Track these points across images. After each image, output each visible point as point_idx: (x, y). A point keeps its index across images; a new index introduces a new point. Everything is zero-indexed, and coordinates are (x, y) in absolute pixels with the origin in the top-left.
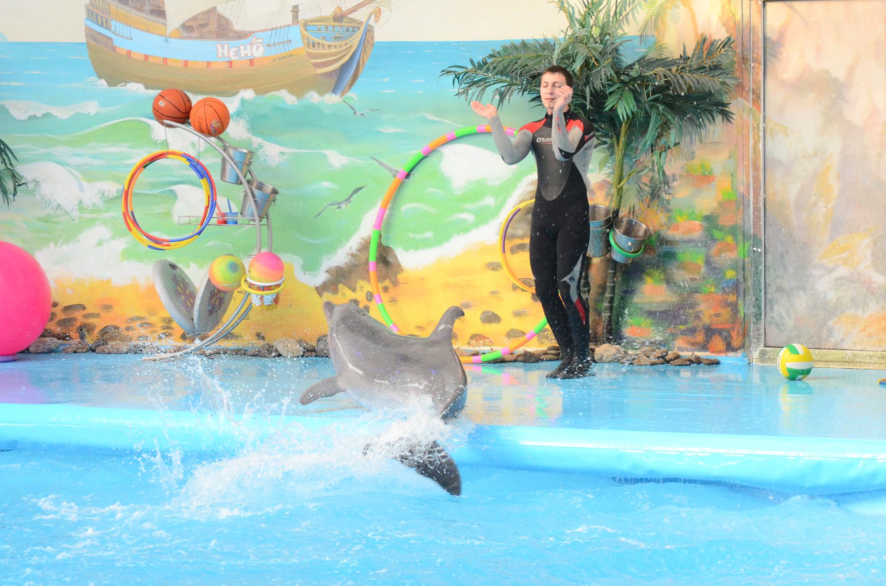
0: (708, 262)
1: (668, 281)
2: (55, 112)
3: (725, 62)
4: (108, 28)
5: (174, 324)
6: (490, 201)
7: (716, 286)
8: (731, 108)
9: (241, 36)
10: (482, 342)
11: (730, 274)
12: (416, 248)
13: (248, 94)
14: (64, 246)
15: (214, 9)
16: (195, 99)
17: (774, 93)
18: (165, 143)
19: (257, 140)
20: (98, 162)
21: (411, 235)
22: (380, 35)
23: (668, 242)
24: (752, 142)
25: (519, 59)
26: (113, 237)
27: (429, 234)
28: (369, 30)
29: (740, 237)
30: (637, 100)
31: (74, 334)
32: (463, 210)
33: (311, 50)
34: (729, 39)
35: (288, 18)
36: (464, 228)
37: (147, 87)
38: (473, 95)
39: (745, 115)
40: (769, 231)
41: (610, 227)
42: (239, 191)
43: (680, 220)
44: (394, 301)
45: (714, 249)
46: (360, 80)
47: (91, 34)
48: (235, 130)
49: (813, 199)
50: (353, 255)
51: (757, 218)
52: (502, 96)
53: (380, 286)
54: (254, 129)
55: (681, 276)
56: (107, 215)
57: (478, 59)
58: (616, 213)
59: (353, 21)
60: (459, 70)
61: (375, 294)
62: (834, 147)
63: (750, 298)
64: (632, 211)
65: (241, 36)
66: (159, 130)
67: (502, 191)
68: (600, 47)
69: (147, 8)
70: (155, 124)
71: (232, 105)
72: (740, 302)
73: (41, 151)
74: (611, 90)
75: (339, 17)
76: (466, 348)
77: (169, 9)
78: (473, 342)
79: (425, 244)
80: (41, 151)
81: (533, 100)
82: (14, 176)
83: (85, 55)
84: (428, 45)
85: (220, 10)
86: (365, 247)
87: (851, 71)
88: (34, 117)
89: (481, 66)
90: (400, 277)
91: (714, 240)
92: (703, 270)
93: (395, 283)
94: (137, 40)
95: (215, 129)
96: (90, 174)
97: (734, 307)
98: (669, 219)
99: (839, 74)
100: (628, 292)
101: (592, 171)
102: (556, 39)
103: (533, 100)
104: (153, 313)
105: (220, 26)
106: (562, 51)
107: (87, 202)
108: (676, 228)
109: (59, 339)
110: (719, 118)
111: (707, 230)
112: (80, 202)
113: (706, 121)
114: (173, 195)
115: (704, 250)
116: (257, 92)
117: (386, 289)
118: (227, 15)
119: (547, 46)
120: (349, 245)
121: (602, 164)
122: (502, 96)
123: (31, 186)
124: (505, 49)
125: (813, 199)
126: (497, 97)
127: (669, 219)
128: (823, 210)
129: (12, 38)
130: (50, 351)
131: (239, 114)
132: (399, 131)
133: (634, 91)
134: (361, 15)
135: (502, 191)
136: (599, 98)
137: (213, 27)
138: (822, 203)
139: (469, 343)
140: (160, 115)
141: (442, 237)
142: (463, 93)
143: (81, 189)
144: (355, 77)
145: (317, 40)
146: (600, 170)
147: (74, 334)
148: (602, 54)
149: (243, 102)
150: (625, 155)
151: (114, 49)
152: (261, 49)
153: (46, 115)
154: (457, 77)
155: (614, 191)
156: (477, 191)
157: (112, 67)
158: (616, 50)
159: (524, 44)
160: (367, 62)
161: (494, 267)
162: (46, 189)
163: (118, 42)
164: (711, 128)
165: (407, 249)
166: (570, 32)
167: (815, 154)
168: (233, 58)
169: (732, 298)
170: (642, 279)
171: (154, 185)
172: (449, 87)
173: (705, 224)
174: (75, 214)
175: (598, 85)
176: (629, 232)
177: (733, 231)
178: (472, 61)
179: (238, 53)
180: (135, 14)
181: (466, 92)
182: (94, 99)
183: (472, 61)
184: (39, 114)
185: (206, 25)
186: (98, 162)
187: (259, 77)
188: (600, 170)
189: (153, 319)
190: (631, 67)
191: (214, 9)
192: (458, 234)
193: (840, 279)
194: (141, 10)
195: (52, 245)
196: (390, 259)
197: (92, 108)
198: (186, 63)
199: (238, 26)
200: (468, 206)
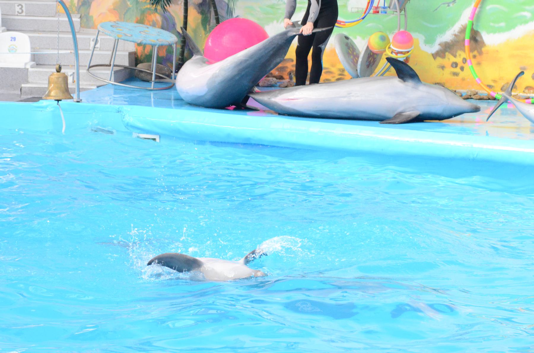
5: (346, 73)
10: (532, 91)
12: (494, 32)
21: (492, 24)
27: (502, 24)
31: (286, 76)
36: (525, 21)
44: (479, 64)
50: (455, 35)
53: (471, 54)
61: (468, 59)
76: (521, 94)
78: (527, 91)
79: (500, 30)
86: (463, 30)
93: (481, 53)
104: (333, 66)
109: (277, 79)
117: (474, 57)
120: (453, 29)
130: (271, 86)
139: (524, 92)
141: (510, 27)
147: (286, 76)
189: (333, 69)
195: (275, 22)
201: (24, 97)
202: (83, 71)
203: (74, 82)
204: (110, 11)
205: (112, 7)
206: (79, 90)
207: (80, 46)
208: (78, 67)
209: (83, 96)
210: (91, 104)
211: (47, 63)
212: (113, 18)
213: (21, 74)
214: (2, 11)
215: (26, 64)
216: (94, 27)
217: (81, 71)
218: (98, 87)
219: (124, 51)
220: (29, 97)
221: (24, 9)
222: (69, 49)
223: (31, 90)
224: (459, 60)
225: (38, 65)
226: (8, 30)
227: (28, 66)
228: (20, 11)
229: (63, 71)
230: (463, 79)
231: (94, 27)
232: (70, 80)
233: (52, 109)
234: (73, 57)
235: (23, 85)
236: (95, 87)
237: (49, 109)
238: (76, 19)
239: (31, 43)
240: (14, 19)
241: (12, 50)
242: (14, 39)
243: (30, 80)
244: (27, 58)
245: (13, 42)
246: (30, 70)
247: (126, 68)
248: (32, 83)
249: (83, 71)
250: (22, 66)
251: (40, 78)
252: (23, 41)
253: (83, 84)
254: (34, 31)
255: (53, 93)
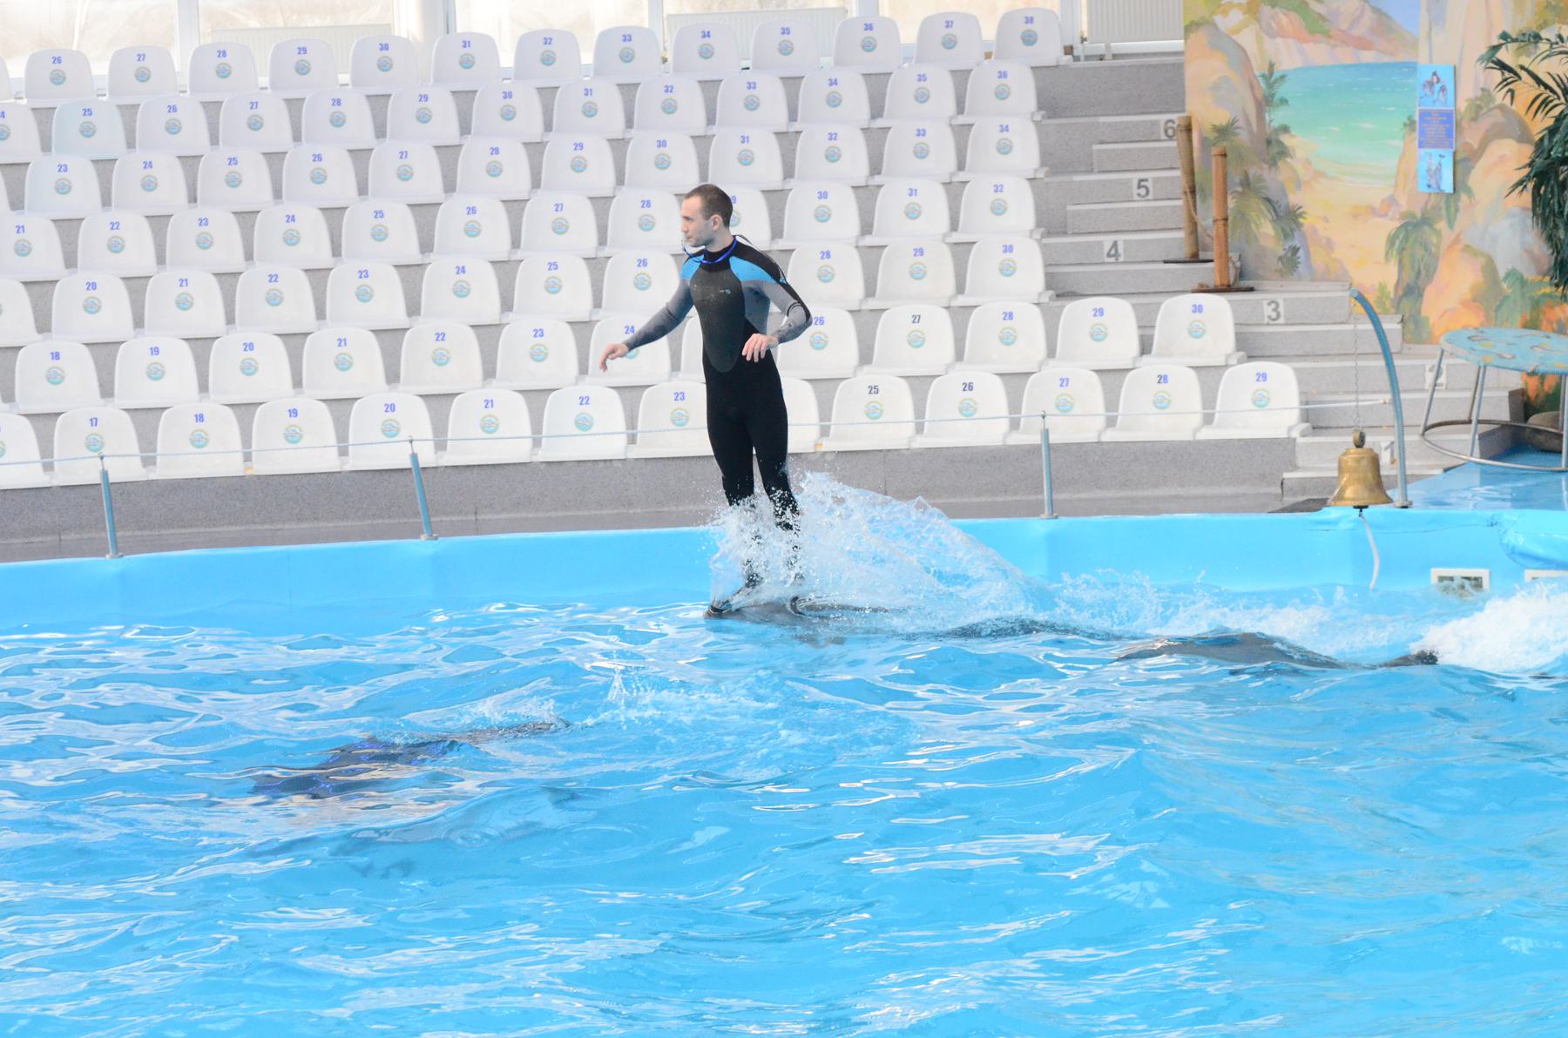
201: (1289, 500)
202: (1412, 438)
203: (1393, 462)
204: (1464, 304)
205: (1469, 296)
206: (1406, 480)
207: (1402, 386)
208: (1402, 426)
209: (1414, 492)
210: (1434, 511)
211: (1334, 424)
212: (1472, 319)
213: (1282, 450)
214: (1235, 317)
215: (1290, 429)
216: (1431, 340)
217: (1407, 438)
218: (1446, 470)
219: (1498, 388)
220: (1301, 499)
221: (1281, 309)
222: (1381, 392)
223: (1303, 485)
225: (1317, 429)
226: (1251, 358)
227: (1295, 434)
228: (1274, 315)
229: (1368, 439)
231: (1431, 340)
232: (1385, 459)
233: (1349, 526)
234: (1389, 412)
235: (1286, 475)
236: (1438, 472)
237: (1341, 526)
238: (1391, 326)
239: (1300, 382)
240: (1263, 334)
241: (1260, 402)
242: (1262, 377)
243: (1300, 463)
244: (1293, 416)
245: (1261, 384)
246: (1300, 440)
247: (1504, 426)
248: (1305, 469)
249: (1412, 438)
250: (1282, 434)
251: (1321, 459)
252: (1283, 379)
253: (1414, 465)
254: (1304, 356)
255: (1349, 493)
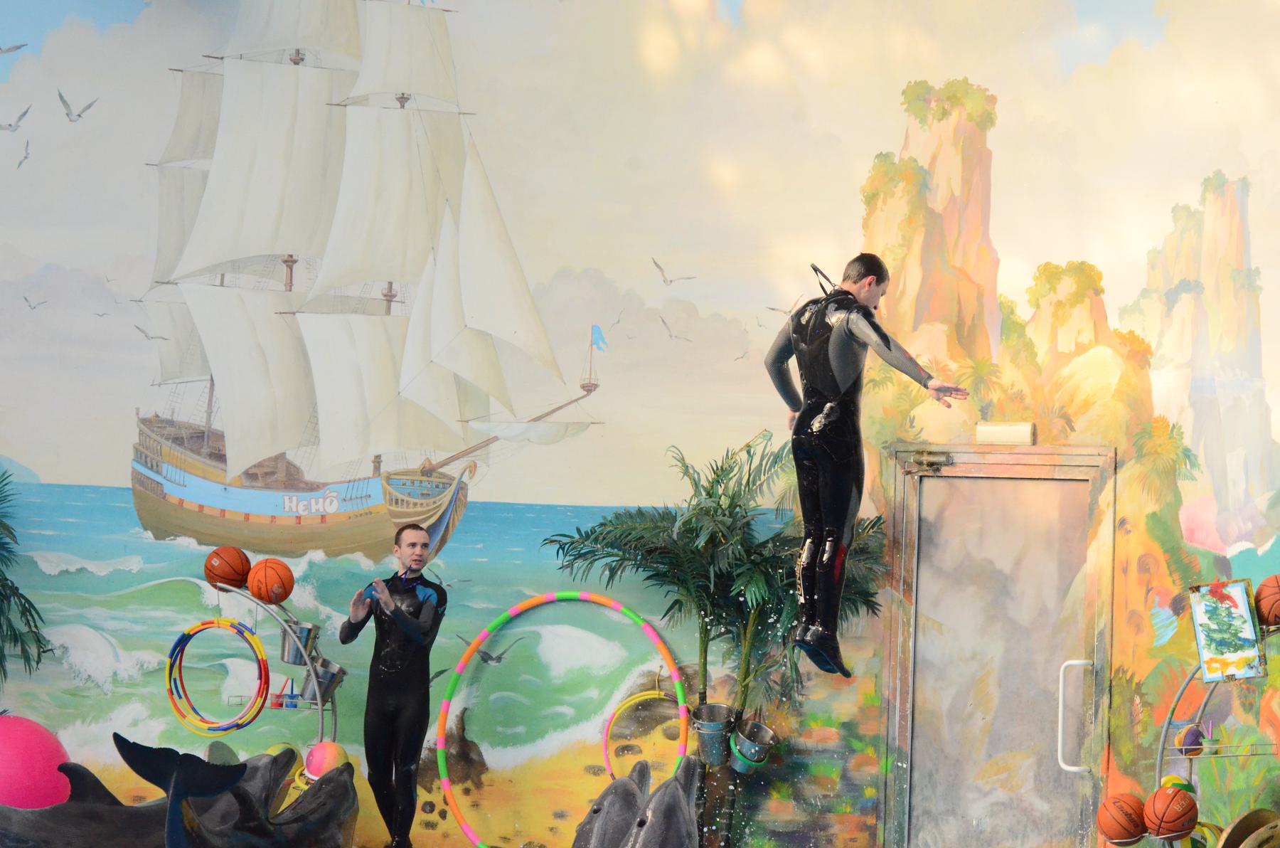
0: (844, 776)
1: (798, 797)
2: (91, 567)
3: (873, 545)
4: (158, 472)
6: (593, 693)
7: (853, 805)
8: (879, 599)
9: (313, 487)
11: (870, 792)
12: (505, 745)
13: (318, 556)
14: (94, 727)
15: (283, 455)
16: (255, 559)
17: (928, 584)
18: (218, 609)
19: (325, 610)
20: (138, 628)
21: (500, 729)
22: (474, 495)
23: (800, 752)
24: (900, 639)
25: (634, 529)
26: (151, 717)
28: (462, 487)
29: (883, 749)
30: (769, 581)
32: (562, 703)
33: (394, 508)
34: (879, 518)
35: (368, 470)
36: (562, 723)
37: (200, 543)
38: (579, 569)
39: (894, 607)
40: (916, 742)
41: (731, 731)
42: (301, 671)
43: (814, 726)
44: (475, 805)
45: (852, 763)
46: (448, 545)
47: (138, 478)
48: (301, 597)
49: (969, 709)
51: (902, 728)
52: (613, 572)
54: (323, 597)
55: (810, 791)
56: (145, 690)
57: (586, 527)
58: (739, 715)
59: (443, 475)
60: (565, 540)
62: (995, 650)
63: (892, 823)
64: (758, 713)
65: (313, 487)
66: (211, 594)
67: (609, 683)
68: (729, 521)
69: (205, 450)
70: (205, 585)
71: (298, 568)
72: (880, 826)
73: (72, 612)
74: (739, 571)
75: (427, 471)
77: (230, 452)
79: (515, 741)
80: (72, 612)
81: (648, 578)
82: (39, 640)
83: (129, 504)
84: (530, 507)
85: (290, 456)
87: (1018, 563)
88: (67, 571)
89: (588, 536)
90: (484, 777)
91: (853, 751)
92: (838, 787)
93: (479, 785)
94: (191, 487)
95: (277, 594)
96: (128, 642)
97: (873, 832)
98: (802, 724)
99: (1004, 565)
100: (753, 808)
101: (713, 664)
102: (681, 509)
103: (648, 578)
105: (289, 474)
106: (684, 524)
107: (123, 675)
108: (809, 734)
110: (863, 610)
111: (844, 738)
112: (115, 674)
113: (849, 613)
114: (224, 670)
115: (840, 763)
116: (331, 554)
118: (297, 462)
119: (668, 516)
121: (726, 655)
122: (613, 572)
123: (58, 653)
124: (618, 516)
125: (969, 709)
126: (607, 573)
127: (802, 724)
128: (980, 723)
129: (45, 479)
131: (305, 578)
132: (492, 606)
133: (766, 574)
134: (453, 470)
135: (609, 683)
136: (725, 580)
137: (281, 475)
138: (978, 715)
140: (212, 576)
141: (534, 735)
142: (567, 566)
143: (117, 657)
144: (443, 541)
145: (400, 497)
146: (724, 663)
148: (731, 529)
149: (311, 564)
150: (752, 646)
151: (164, 496)
152: (335, 503)
153: (81, 570)
154: (562, 547)
155: (739, 689)
156: (580, 681)
157: (160, 518)
158: (748, 524)
159: (640, 512)
160: (457, 524)
161: (596, 771)
162: (75, 657)
163: (168, 488)
164: (853, 620)
165: (493, 745)
166: (694, 502)
167: (973, 657)
168: (301, 513)
169: (870, 820)
170: (768, 795)
171: (203, 658)
172: (552, 559)
173: (843, 732)
174: (108, 687)
175: (724, 565)
176: (753, 736)
177: (875, 742)
178: (578, 530)
179: (308, 507)
180: (191, 458)
181: (571, 565)
182: (136, 554)
183: (578, 530)
184: (72, 569)
185: (273, 473)
186: (138, 628)
187: (333, 539)
188: (724, 663)
190: (764, 544)
191: (283, 455)
192: (555, 730)
193: (996, 804)
194: (199, 453)
196: (474, 756)
197: (134, 564)
198: (247, 516)
199: (309, 476)
200: (567, 698)
224: (435, 798)
230: (445, 836)
